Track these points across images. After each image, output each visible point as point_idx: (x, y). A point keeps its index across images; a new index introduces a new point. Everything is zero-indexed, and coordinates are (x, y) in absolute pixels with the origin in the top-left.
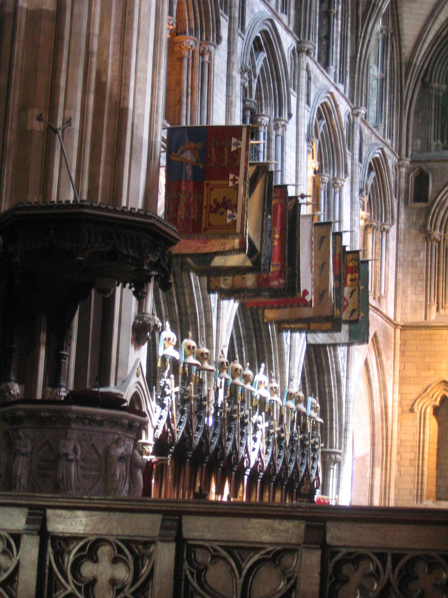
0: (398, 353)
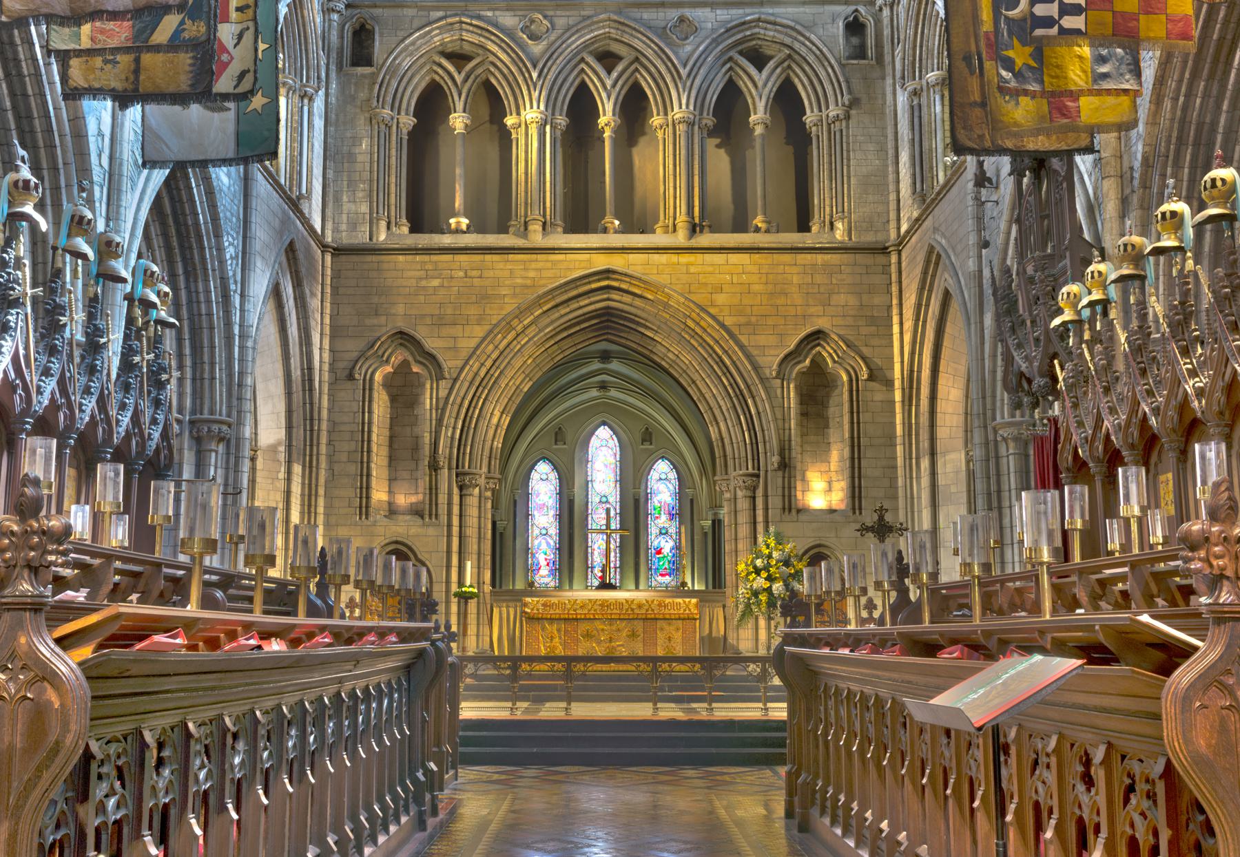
0: (328, 290)
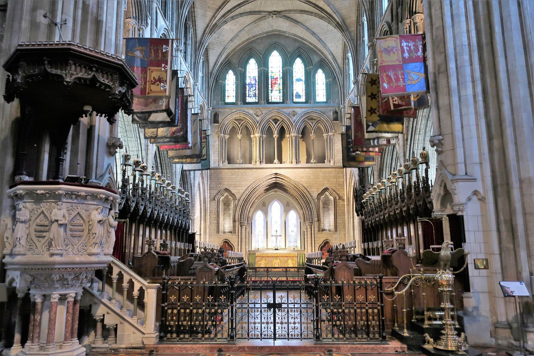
0: (209, 178)
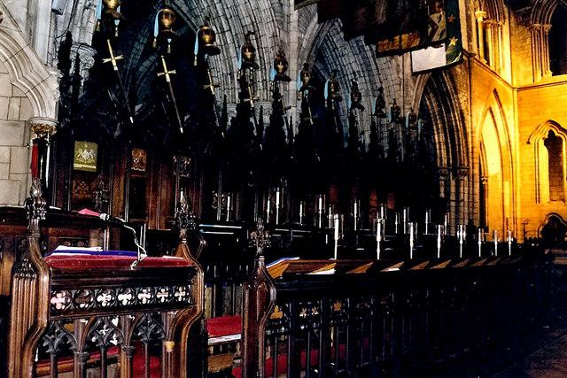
0: (516, 106)
